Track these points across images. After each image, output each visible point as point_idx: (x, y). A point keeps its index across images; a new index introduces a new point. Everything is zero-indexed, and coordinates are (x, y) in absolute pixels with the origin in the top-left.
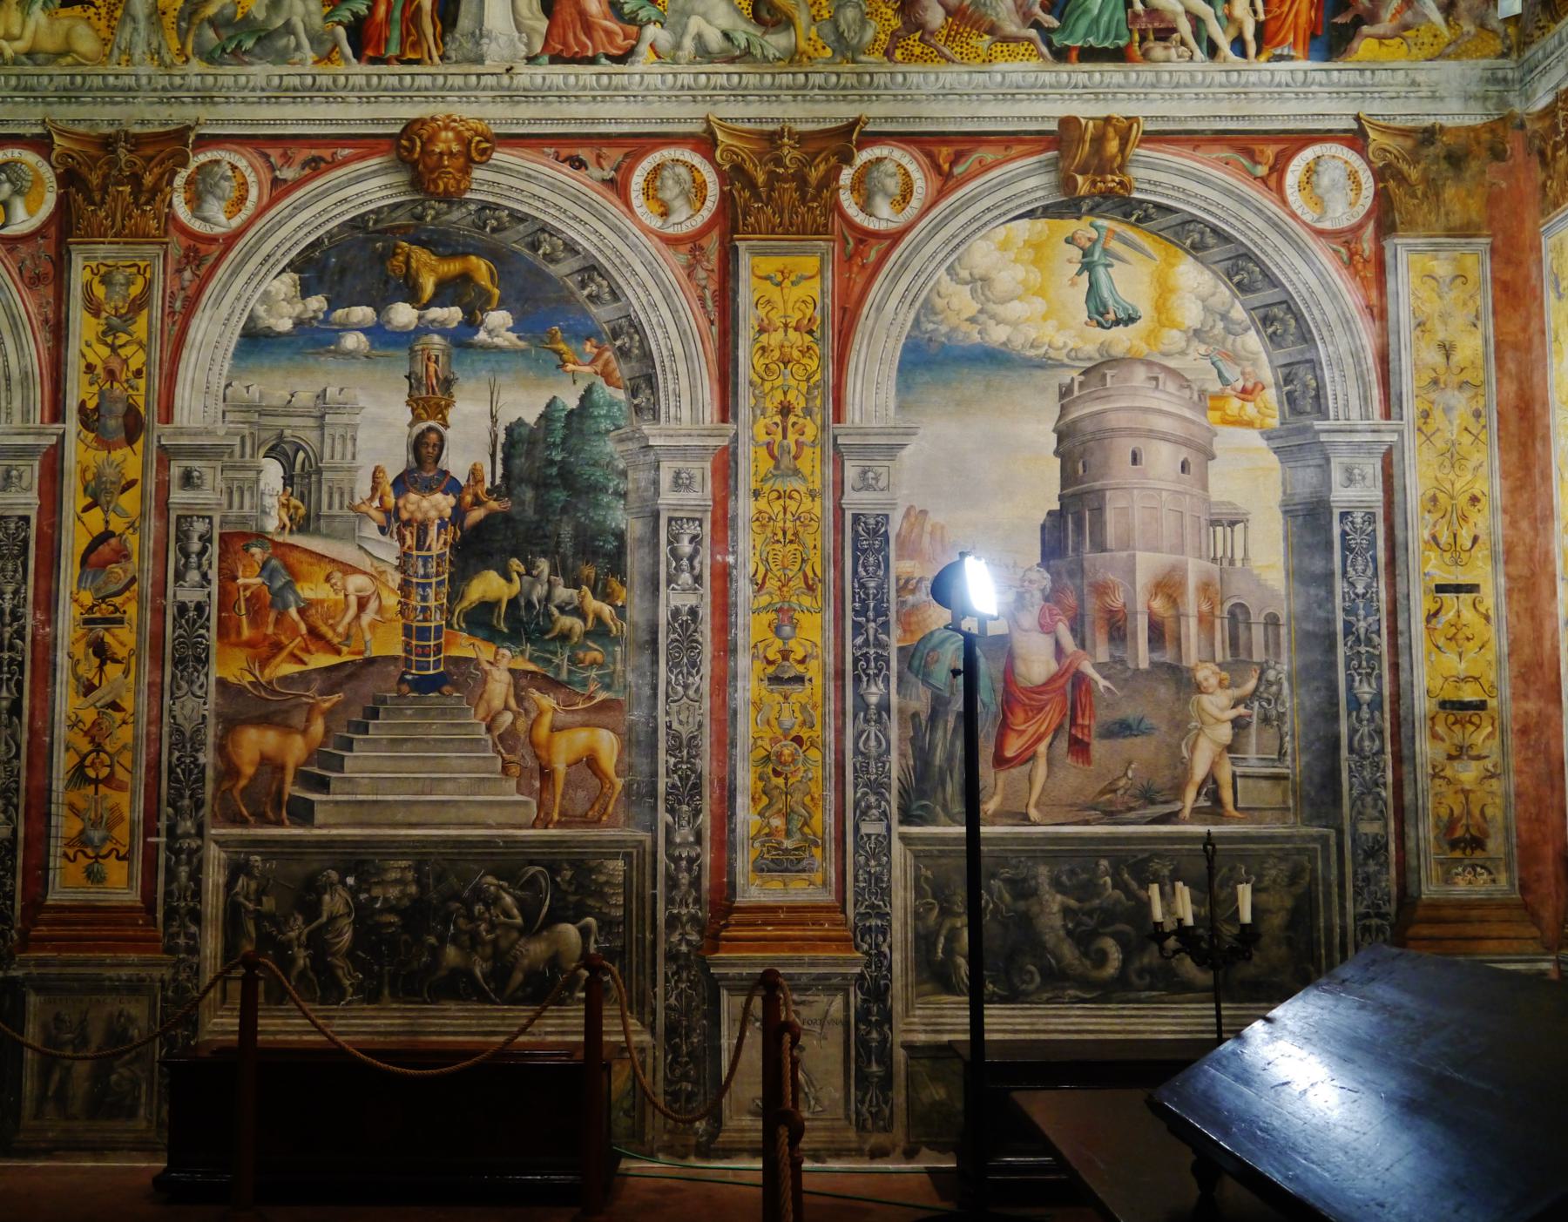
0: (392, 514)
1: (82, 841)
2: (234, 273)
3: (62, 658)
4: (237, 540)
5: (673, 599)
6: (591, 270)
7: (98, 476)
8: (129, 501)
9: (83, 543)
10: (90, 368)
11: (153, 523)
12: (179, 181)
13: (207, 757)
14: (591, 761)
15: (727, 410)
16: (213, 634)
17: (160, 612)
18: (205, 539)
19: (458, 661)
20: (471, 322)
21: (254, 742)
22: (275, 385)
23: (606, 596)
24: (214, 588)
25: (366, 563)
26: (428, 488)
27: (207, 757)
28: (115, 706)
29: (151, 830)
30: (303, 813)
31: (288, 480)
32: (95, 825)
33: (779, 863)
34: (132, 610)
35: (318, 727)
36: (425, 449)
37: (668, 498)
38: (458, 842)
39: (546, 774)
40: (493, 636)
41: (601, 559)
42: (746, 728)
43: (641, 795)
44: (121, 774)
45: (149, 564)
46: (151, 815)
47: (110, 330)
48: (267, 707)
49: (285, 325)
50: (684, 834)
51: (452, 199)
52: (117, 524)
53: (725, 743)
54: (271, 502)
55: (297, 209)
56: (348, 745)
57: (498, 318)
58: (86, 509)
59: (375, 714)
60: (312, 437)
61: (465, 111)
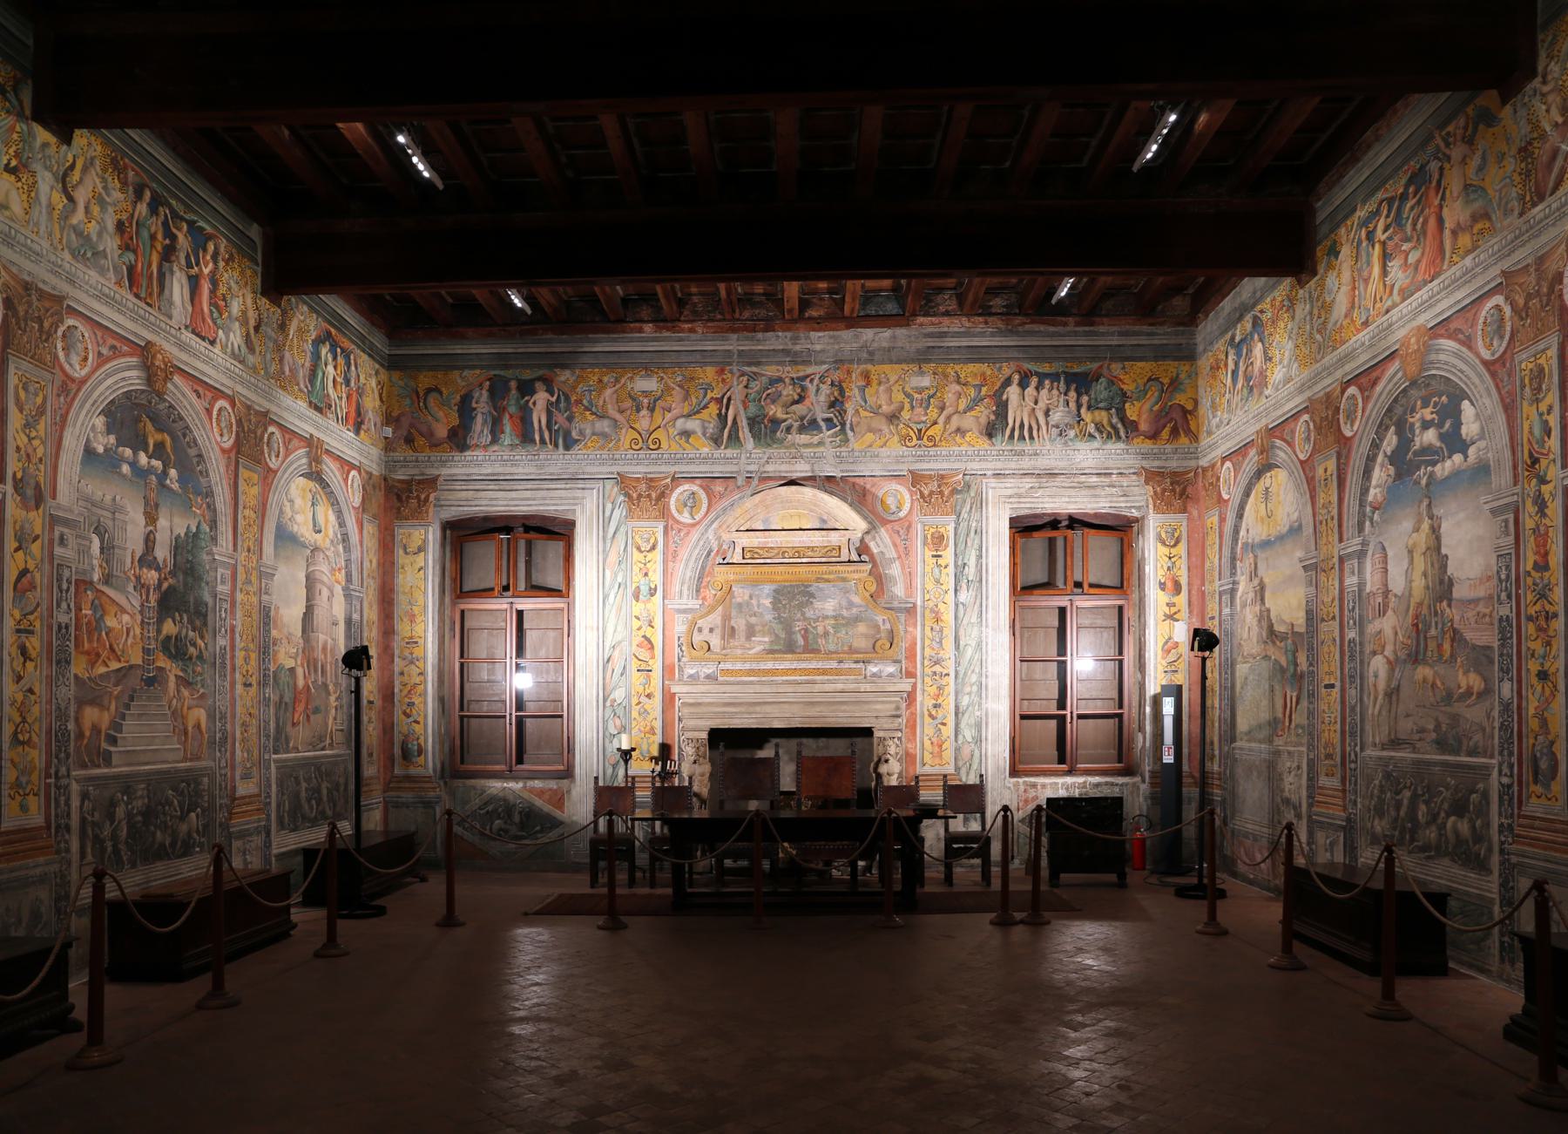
0: (138, 578)
1: (17, 785)
2: (82, 407)
3: (6, 658)
4: (83, 584)
5: (222, 642)
6: (200, 456)
7: (22, 528)
8: (35, 548)
9: (16, 573)
10: (18, 449)
11: (47, 566)
12: (60, 333)
13: (71, 726)
14: (198, 726)
15: (235, 545)
16: (72, 645)
17: (50, 628)
18: (69, 582)
19: (161, 669)
20: (165, 473)
21: (91, 714)
22: (101, 489)
23: (202, 637)
24: (73, 615)
25: (128, 607)
26: (150, 567)
27: (71, 726)
28: (31, 691)
29: (48, 776)
30: (107, 759)
31: (102, 549)
32: (23, 773)
33: (246, 776)
34: (38, 624)
35: (113, 707)
36: (149, 541)
37: (220, 588)
38: (159, 772)
39: (186, 733)
40: (171, 657)
41: (199, 616)
42: (239, 709)
43: (212, 742)
44: (35, 738)
45: (45, 595)
46: (48, 764)
47: (27, 425)
48: (90, 694)
49: (101, 449)
50: (223, 764)
51: (160, 395)
52: (31, 566)
53: (233, 716)
54: (95, 562)
55: (109, 376)
56: (123, 717)
57: (173, 472)
58: (16, 550)
59: (132, 699)
60: (110, 523)
61: (166, 346)
